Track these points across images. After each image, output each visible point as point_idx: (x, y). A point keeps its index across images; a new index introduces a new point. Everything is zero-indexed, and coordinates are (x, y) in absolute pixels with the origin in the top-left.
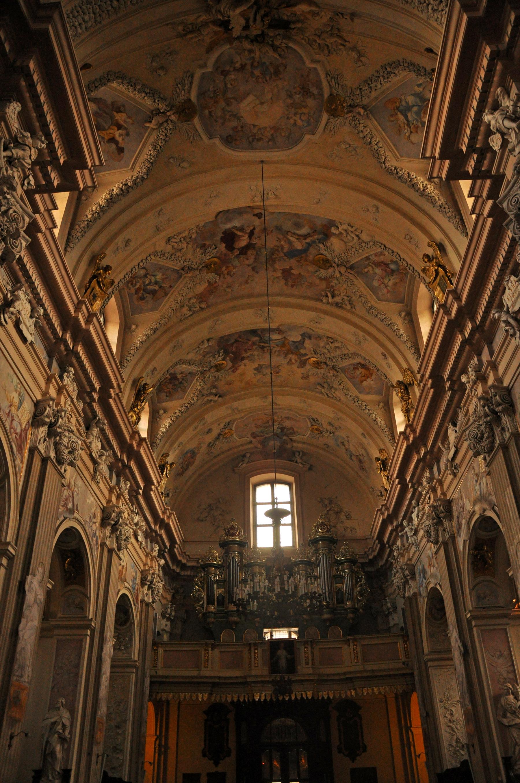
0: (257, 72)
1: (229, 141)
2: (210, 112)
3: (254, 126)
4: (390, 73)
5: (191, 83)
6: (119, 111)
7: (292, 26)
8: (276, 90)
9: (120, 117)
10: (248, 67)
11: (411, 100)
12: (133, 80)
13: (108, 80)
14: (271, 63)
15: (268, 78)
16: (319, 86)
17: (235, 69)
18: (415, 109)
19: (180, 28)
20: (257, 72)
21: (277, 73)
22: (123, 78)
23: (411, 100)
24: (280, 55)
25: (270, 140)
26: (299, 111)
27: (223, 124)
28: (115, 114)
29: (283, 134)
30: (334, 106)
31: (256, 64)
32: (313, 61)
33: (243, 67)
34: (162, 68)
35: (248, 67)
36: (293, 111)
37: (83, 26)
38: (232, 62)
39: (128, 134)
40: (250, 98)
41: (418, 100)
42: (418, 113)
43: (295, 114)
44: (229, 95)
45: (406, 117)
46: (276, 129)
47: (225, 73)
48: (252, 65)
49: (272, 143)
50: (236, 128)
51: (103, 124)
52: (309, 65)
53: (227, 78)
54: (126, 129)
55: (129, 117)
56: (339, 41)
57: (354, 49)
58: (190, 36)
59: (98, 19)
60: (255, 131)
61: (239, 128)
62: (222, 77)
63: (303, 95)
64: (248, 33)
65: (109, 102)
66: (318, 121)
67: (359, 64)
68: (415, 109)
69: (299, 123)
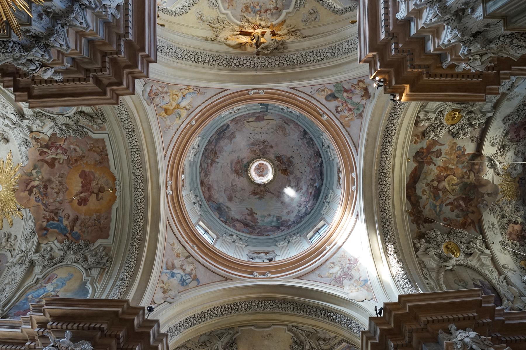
0: (258, 8)
4: (182, 9)
5: (296, 4)
7: (238, 33)
12: (328, 9)
13: (342, 10)
14: (250, 13)
15: (252, 5)
17: (271, 10)
19: (298, 34)
20: (258, 8)
21: (247, 8)
22: (333, 10)
31: (259, 13)
32: (227, 14)
33: (266, 11)
34: (311, 14)
35: (263, 11)
37: (350, 43)
38: (272, 14)
47: (276, 8)
48: (261, 12)
52: (229, 12)
53: (275, 6)
56: (212, 25)
57: (204, 21)
58: (293, 30)
59: (341, 45)
62: (278, 6)
64: (263, 30)
67: (200, 13)
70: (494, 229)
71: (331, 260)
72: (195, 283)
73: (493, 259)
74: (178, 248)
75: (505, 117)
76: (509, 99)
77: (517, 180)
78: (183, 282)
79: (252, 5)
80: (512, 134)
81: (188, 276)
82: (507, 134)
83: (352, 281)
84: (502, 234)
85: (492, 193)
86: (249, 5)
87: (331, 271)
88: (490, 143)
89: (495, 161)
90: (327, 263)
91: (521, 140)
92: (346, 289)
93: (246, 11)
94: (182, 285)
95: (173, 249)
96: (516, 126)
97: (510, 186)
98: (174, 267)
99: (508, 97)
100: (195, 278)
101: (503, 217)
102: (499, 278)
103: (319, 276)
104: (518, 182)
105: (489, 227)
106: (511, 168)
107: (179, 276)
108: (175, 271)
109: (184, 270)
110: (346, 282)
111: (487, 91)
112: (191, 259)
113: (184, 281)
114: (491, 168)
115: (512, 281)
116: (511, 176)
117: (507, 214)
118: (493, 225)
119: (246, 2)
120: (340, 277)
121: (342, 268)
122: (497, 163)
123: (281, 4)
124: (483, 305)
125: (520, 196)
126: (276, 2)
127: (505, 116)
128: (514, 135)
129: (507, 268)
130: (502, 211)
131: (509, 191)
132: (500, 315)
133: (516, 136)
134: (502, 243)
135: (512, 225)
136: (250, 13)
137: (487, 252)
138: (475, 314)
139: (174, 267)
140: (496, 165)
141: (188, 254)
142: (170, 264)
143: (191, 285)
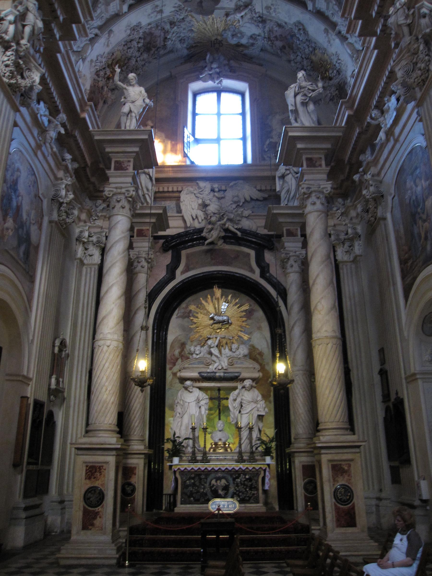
70: (155, 13)
73: (117, 16)
75: (303, 25)
76: (326, 31)
77: (219, 38)
80: (278, 31)
82: (279, 26)
84: (149, 24)
85: (202, 7)
88: (270, 5)
89: (246, 11)
91: (269, 43)
96: (289, 37)
97: (211, 30)
99: (330, 31)
101: (172, 23)
102: (95, 28)
104: (216, 39)
105: (157, 6)
106: (234, 31)
111: (354, 21)
114: (236, 5)
115: (96, 45)
116: (225, 30)
117: (175, 28)
118: (161, 11)
122: (243, 14)
124: (74, 26)
125: (198, 42)
127: (305, 25)
128: (278, 34)
129: (109, 36)
130: (180, 22)
131: (204, 29)
132: (65, 47)
133: (276, 37)
134: (139, 25)
135: (162, 34)
137: (125, 8)
138: (61, 18)
140: (240, 12)
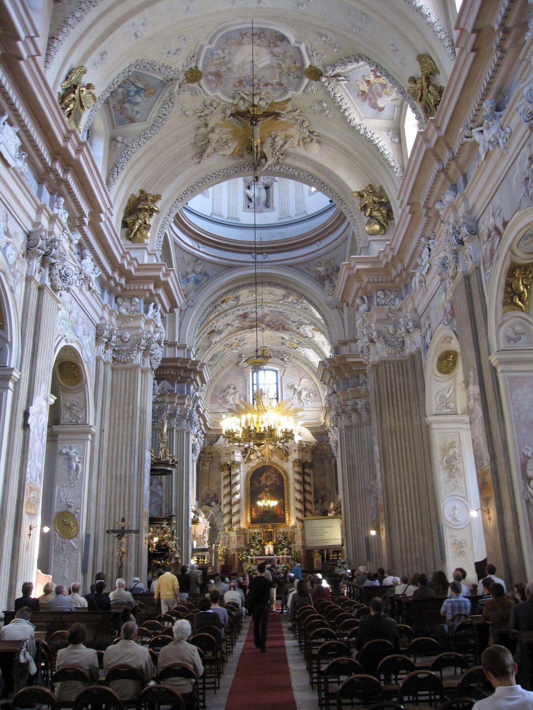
1: (283, 38)
2: (295, 63)
3: (259, 45)
6: (363, 92)
8: (241, 71)
9: (364, 87)
10: (262, 84)
11: (138, 99)
14: (245, 86)
15: (247, 78)
16: (208, 81)
17: (272, 85)
18: (132, 94)
23: (138, 99)
24: (239, 94)
25: (245, 34)
26: (221, 60)
27: (285, 52)
28: (367, 92)
29: (233, 41)
30: (194, 76)
33: (266, 85)
35: (262, 84)
36: (227, 59)
38: (274, 89)
39: (364, 76)
40: (261, 66)
41: (133, 100)
42: (128, 92)
43: (224, 57)
44: (278, 70)
45: (136, 87)
46: (240, 44)
48: (259, 85)
49: (242, 34)
50: (275, 46)
51: (379, 87)
54: (364, 79)
55: (358, 85)
56: (200, 114)
60: (258, 42)
61: (272, 45)
62: (282, 82)
63: (219, 72)
65: (367, 101)
66: (206, 57)
67: (184, 109)
68: (132, 94)
69: (220, 52)
71: (319, 260)
72: (206, 278)
74: (187, 258)
78: (197, 282)
79: (247, 78)
81: (199, 275)
83: (331, 285)
86: (243, 79)
87: (318, 268)
90: (316, 261)
92: (326, 288)
93: (240, 85)
94: (197, 284)
95: (184, 261)
98: (187, 274)
100: (206, 274)
103: (307, 268)
107: (193, 279)
108: (189, 277)
109: (195, 272)
110: (327, 283)
112: (199, 262)
113: (197, 280)
119: (238, 75)
120: (323, 276)
121: (326, 270)
123: (286, 81)
126: (280, 77)
136: (245, 86)
139: (187, 274)
141: (195, 259)
142: (184, 274)
143: (203, 282)
